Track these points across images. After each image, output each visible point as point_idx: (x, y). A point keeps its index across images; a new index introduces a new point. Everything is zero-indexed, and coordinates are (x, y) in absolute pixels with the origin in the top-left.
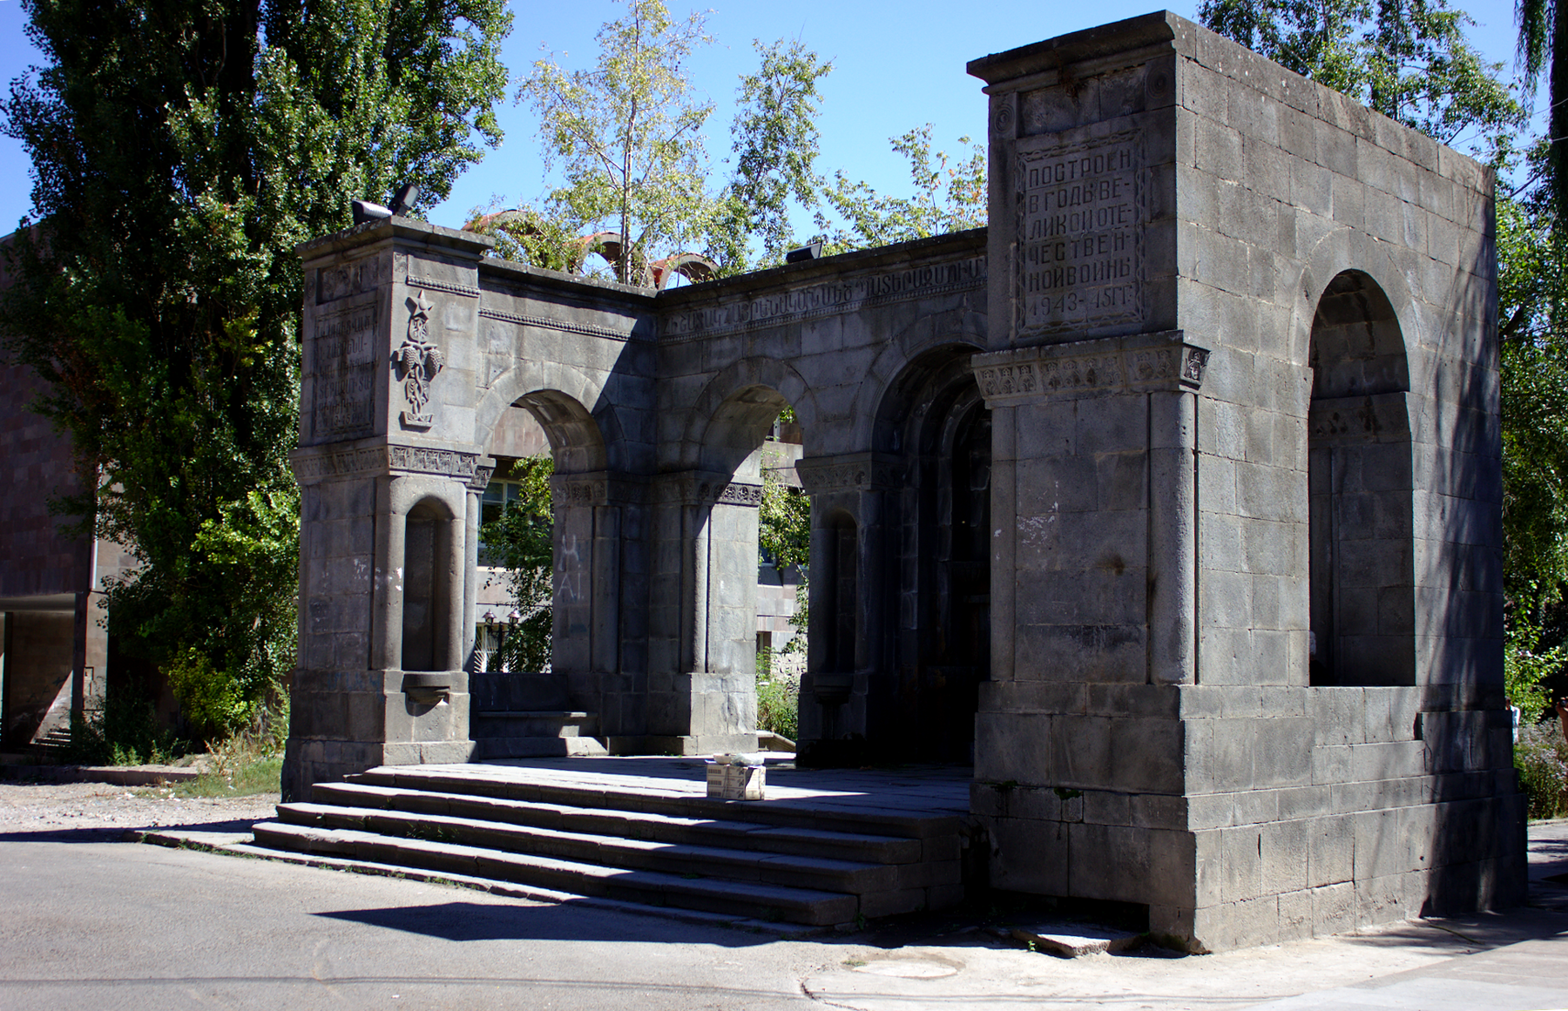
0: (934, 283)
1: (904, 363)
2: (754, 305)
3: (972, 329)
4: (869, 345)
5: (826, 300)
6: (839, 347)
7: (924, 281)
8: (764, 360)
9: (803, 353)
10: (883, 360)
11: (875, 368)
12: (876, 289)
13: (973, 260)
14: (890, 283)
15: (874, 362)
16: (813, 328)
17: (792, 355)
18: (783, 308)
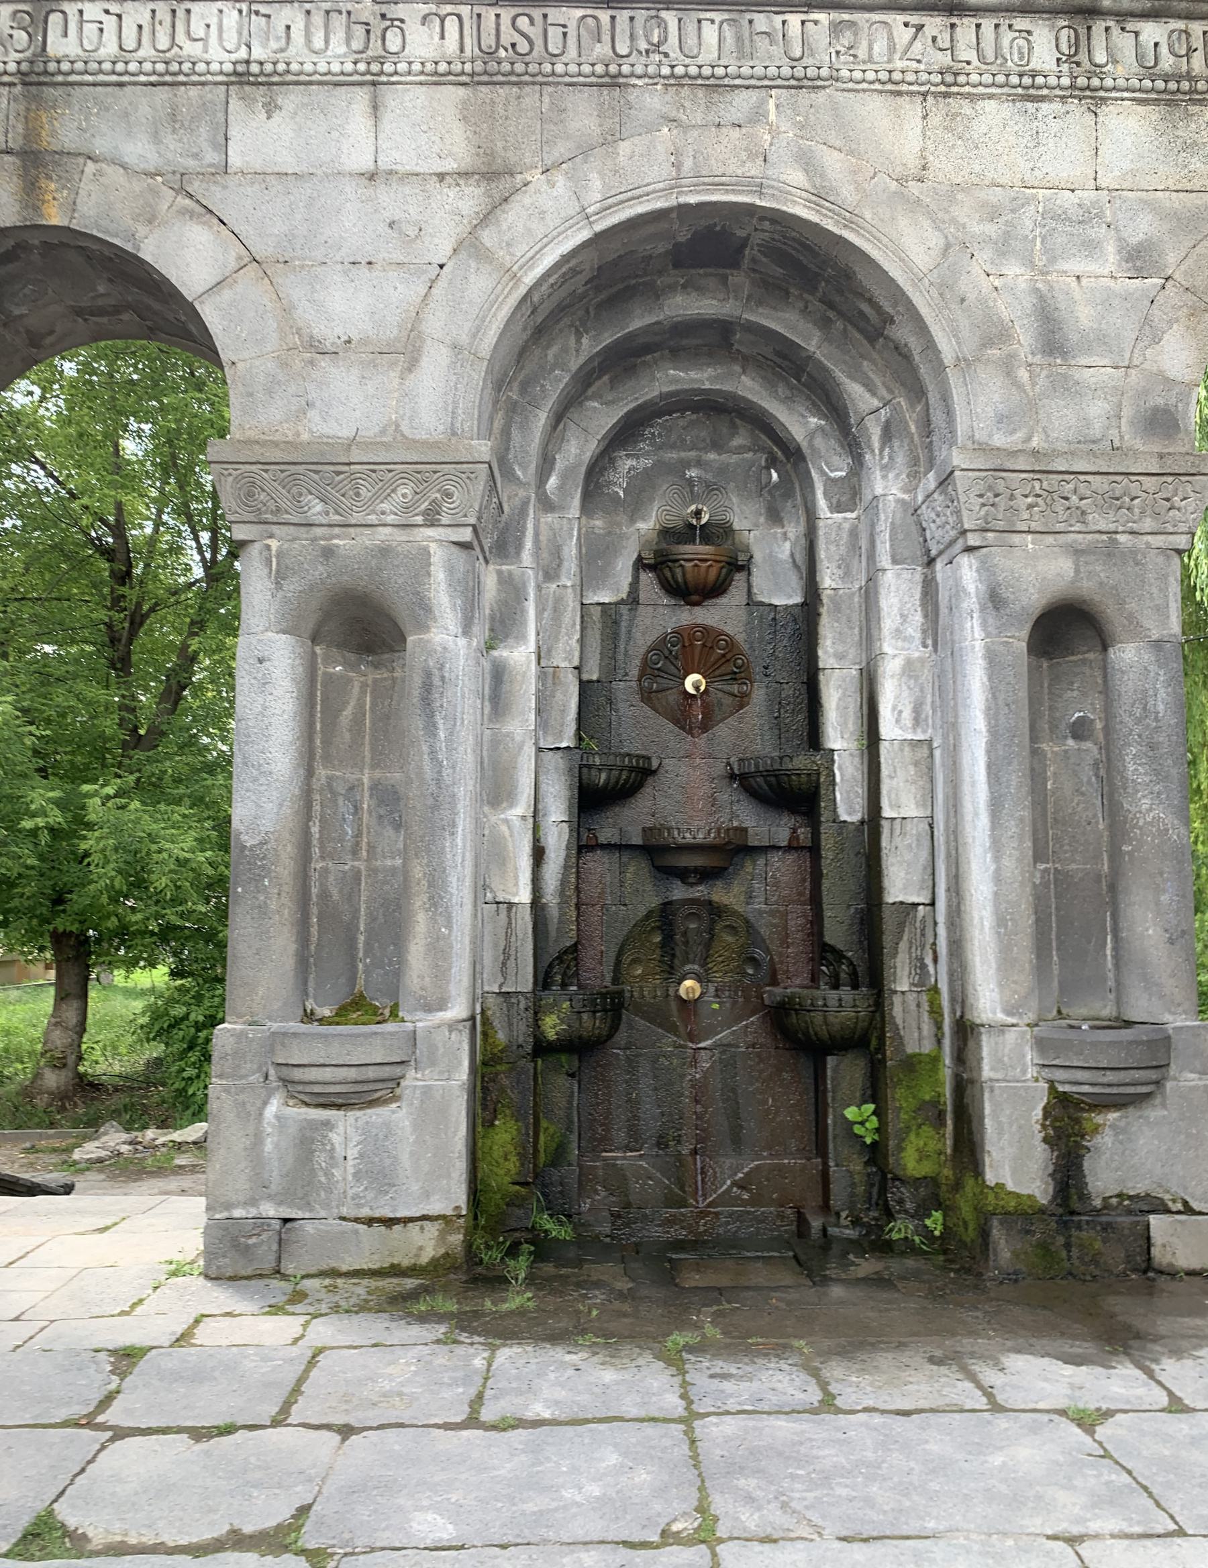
0: (675, 54)
1: (585, 235)
2: (55, 18)
3: (797, 177)
4: (466, 175)
5: (318, 43)
6: (366, 163)
7: (643, 46)
8: (90, 167)
9: (235, 160)
10: (514, 216)
11: (488, 237)
12: (488, 41)
13: (794, 20)
14: (535, 32)
15: (486, 218)
16: (271, 108)
17: (191, 163)
18: (163, 42)
